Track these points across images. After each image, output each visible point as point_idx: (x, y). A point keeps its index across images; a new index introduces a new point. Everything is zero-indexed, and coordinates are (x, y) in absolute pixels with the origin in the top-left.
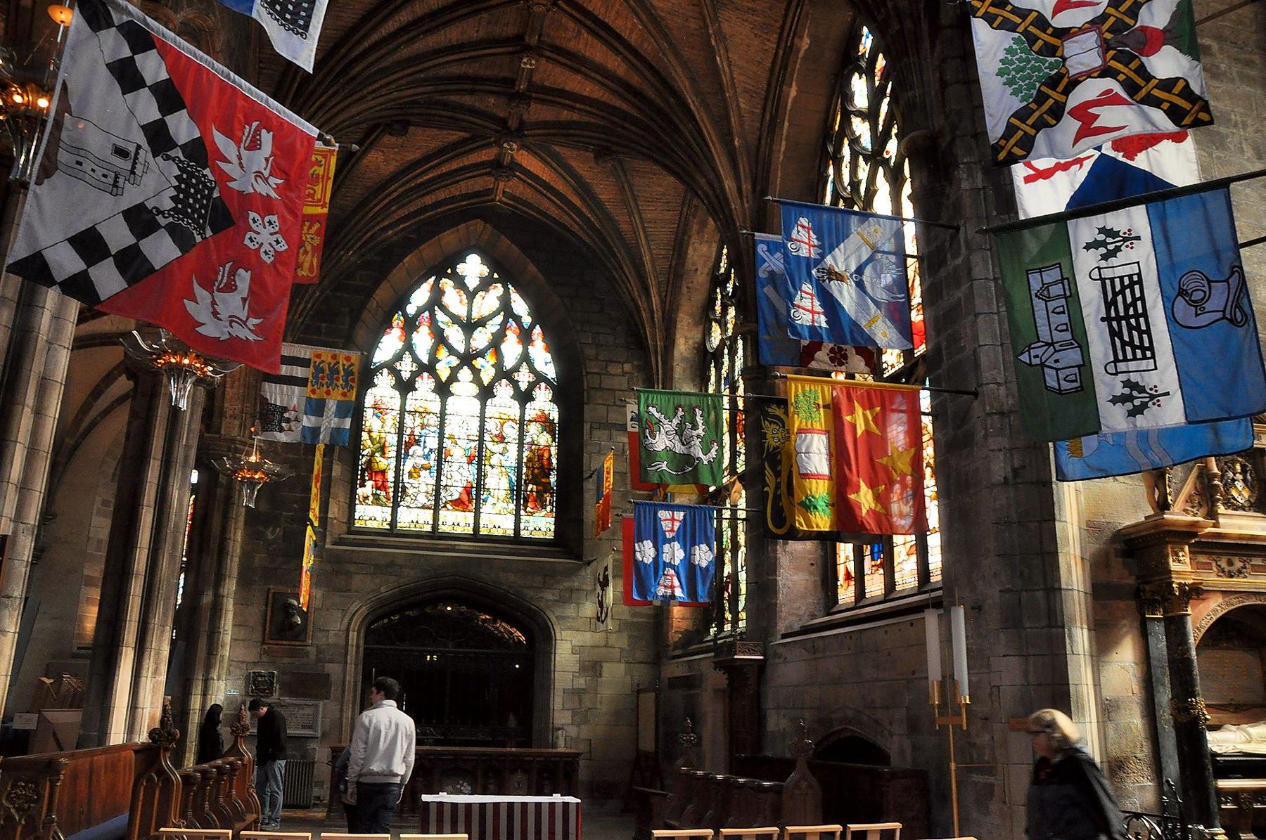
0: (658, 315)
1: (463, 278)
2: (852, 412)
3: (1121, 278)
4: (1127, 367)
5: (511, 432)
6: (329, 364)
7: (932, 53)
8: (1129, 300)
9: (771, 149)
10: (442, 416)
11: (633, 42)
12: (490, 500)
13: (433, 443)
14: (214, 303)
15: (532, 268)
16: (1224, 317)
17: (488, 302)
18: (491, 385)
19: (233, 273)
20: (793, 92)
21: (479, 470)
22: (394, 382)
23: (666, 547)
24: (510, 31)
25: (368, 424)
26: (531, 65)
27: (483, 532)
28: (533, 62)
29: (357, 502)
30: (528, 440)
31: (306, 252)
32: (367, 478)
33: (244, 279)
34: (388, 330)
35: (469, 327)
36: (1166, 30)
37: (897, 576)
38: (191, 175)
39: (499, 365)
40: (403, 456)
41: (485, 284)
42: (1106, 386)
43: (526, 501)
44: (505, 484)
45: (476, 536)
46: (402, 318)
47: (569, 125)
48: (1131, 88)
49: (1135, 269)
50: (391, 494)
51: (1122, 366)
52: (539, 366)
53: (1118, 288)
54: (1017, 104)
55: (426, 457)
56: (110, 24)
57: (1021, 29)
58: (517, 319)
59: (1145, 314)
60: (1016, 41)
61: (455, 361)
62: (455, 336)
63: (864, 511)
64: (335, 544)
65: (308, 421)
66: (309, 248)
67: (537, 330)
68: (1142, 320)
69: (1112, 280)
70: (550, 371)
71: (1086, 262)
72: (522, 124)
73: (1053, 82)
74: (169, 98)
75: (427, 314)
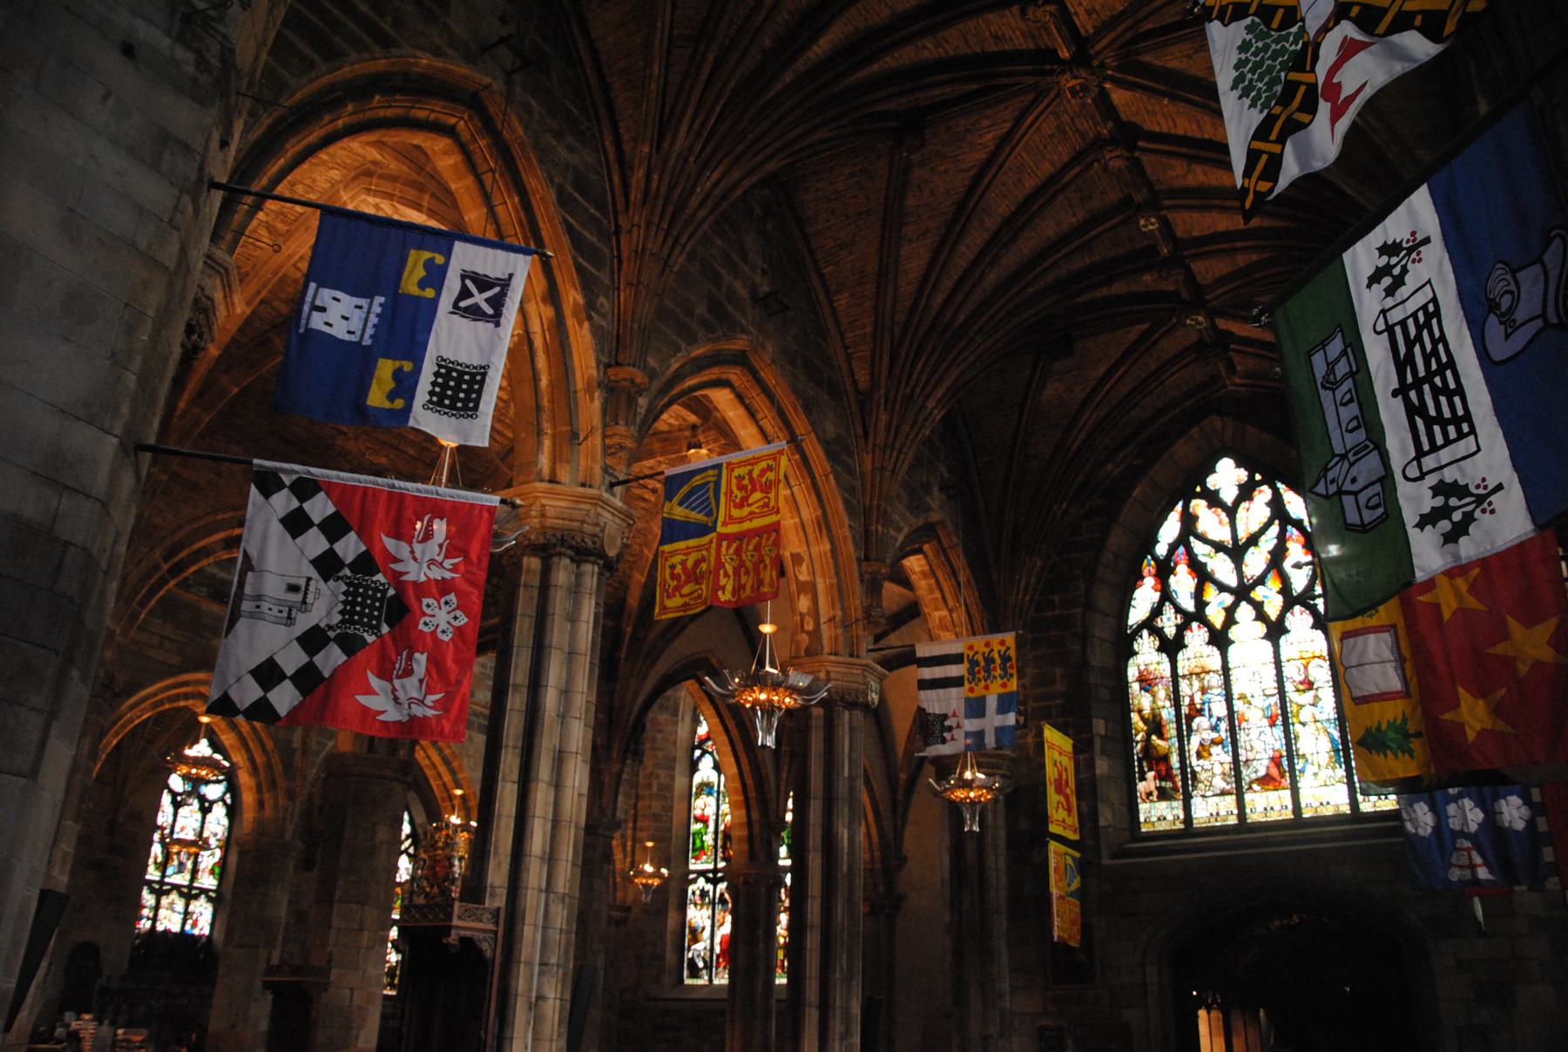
1: (1217, 492)
3: (1414, 315)
4: (1439, 461)
6: (984, 653)
10: (1226, 670)
12: (1310, 770)
13: (1219, 709)
14: (394, 690)
16: (1547, 325)
18: (1282, 617)
19: (410, 658)
21: (1287, 732)
22: (1157, 643)
23: (1452, 809)
24: (1113, 197)
25: (1136, 702)
26: (1152, 224)
27: (1307, 814)
28: (1153, 220)
29: (1139, 800)
31: (726, 575)
32: (1146, 769)
33: (421, 659)
34: (1139, 583)
35: (1236, 552)
38: (357, 587)
39: (1285, 590)
40: (1185, 733)
41: (1246, 492)
44: (1325, 745)
46: (1152, 563)
49: (1427, 294)
50: (1180, 784)
51: (1429, 462)
54: (1256, 117)
55: (1214, 728)
58: (1298, 524)
61: (1228, 599)
62: (1221, 567)
63: (1471, 736)
64: (1115, 856)
65: (970, 725)
66: (768, 561)
75: (1181, 549)
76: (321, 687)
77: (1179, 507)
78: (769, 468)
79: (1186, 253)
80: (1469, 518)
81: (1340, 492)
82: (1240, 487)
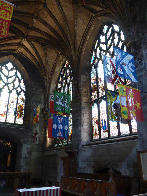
0: (48, 80)
5: (15, 101)
7: (134, 27)
9: (82, 48)
11: (58, 20)
15: (23, 67)
17: (13, 73)
18: (12, 90)
20: (88, 37)
23: (59, 126)
24: (32, 12)
27: (7, 122)
30: (18, 103)
35: (8, 78)
37: (111, 134)
39: (14, 86)
41: (12, 69)
43: (17, 116)
52: (22, 88)
58: (18, 78)
61: (4, 84)
66: (5, 28)
67: (22, 81)
70: (25, 89)
72: (27, 36)
78: (8, 7)
79: (33, 29)
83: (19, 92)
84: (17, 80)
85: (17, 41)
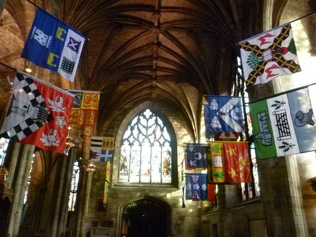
2: (228, 150)
3: (281, 114)
5: (159, 156)
8: (283, 120)
19: (53, 130)
20: (222, 63)
23: (194, 185)
24: (149, 54)
27: (152, 182)
33: (56, 131)
35: (147, 128)
36: (288, 48)
39: (155, 138)
41: (151, 117)
42: (278, 144)
45: (150, 183)
47: (168, 76)
48: (280, 63)
49: (284, 111)
51: (282, 138)
53: (280, 117)
54: (252, 70)
56: (23, 79)
57: (252, 50)
58: (160, 126)
59: (287, 124)
60: (251, 53)
62: (143, 130)
63: (233, 176)
65: (102, 156)
67: (165, 128)
68: (287, 125)
69: (279, 115)
70: (169, 139)
71: (271, 110)
72: (156, 76)
73: (261, 63)
74: (37, 93)
75: (136, 126)
76: (31, 135)
77: (137, 117)
80: (288, 149)
81: (261, 138)
82: (150, 116)
83: (162, 143)
84: (159, 128)
85: (149, 84)
